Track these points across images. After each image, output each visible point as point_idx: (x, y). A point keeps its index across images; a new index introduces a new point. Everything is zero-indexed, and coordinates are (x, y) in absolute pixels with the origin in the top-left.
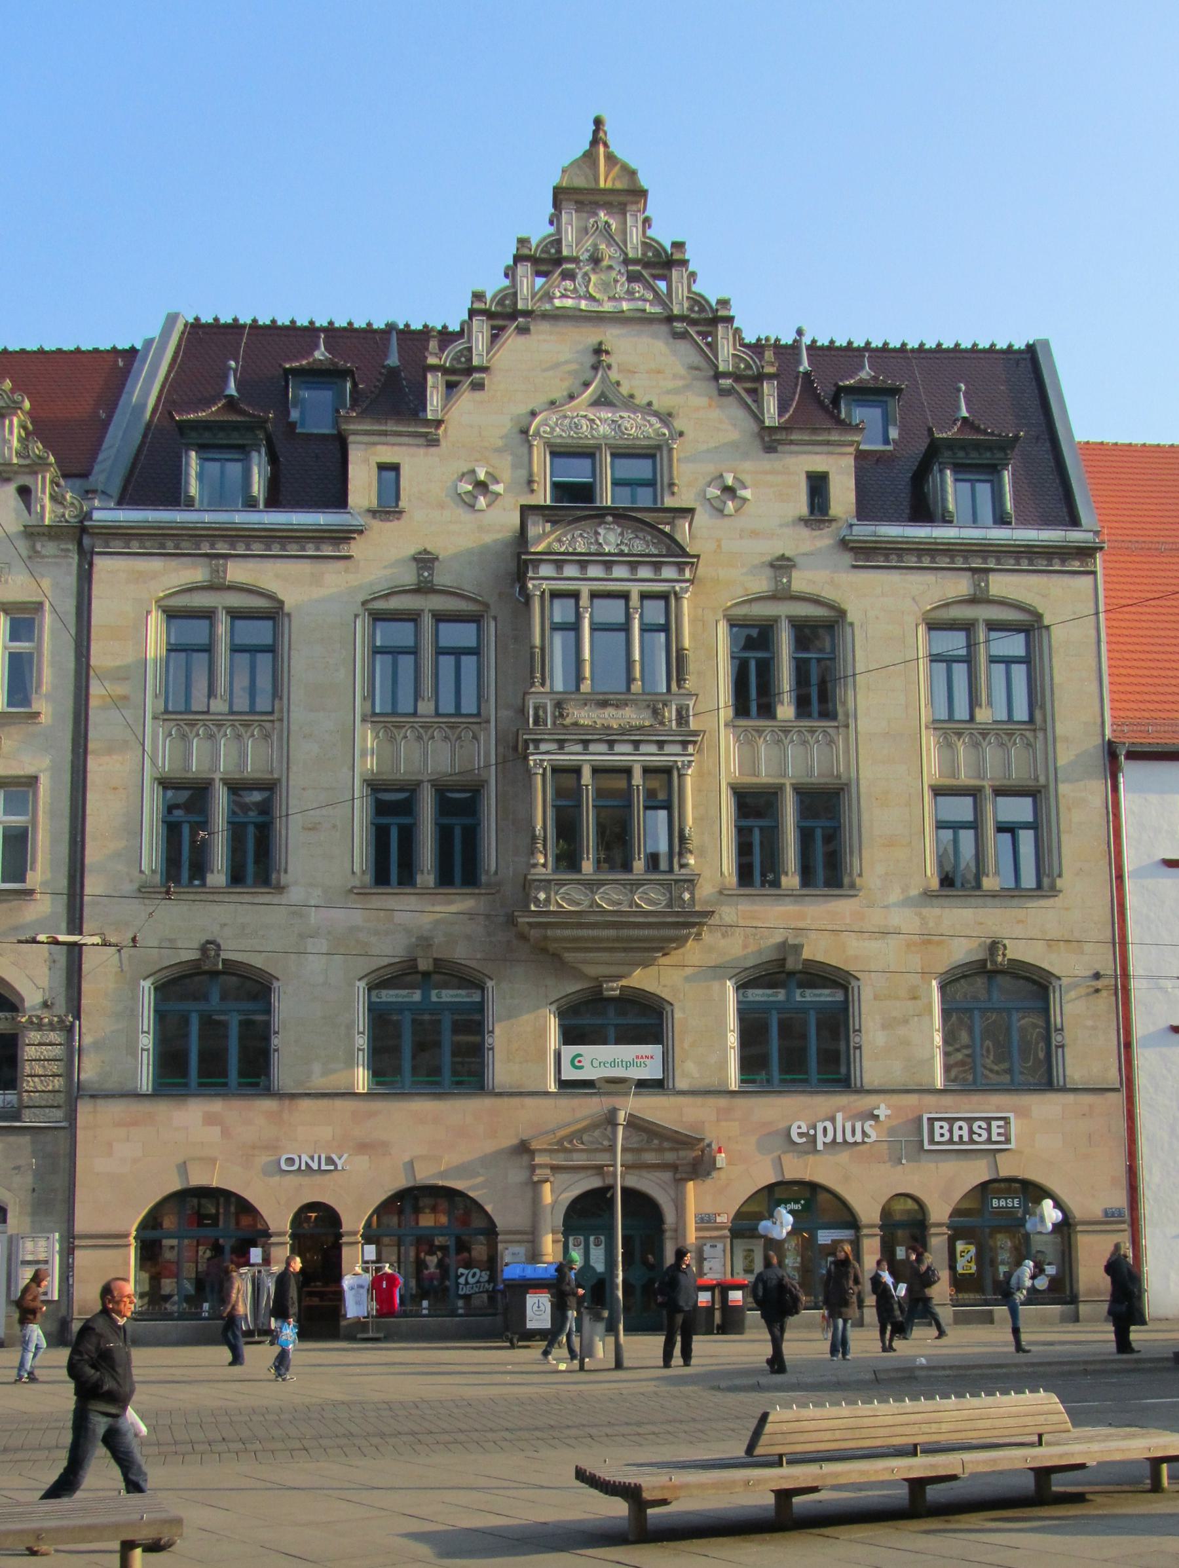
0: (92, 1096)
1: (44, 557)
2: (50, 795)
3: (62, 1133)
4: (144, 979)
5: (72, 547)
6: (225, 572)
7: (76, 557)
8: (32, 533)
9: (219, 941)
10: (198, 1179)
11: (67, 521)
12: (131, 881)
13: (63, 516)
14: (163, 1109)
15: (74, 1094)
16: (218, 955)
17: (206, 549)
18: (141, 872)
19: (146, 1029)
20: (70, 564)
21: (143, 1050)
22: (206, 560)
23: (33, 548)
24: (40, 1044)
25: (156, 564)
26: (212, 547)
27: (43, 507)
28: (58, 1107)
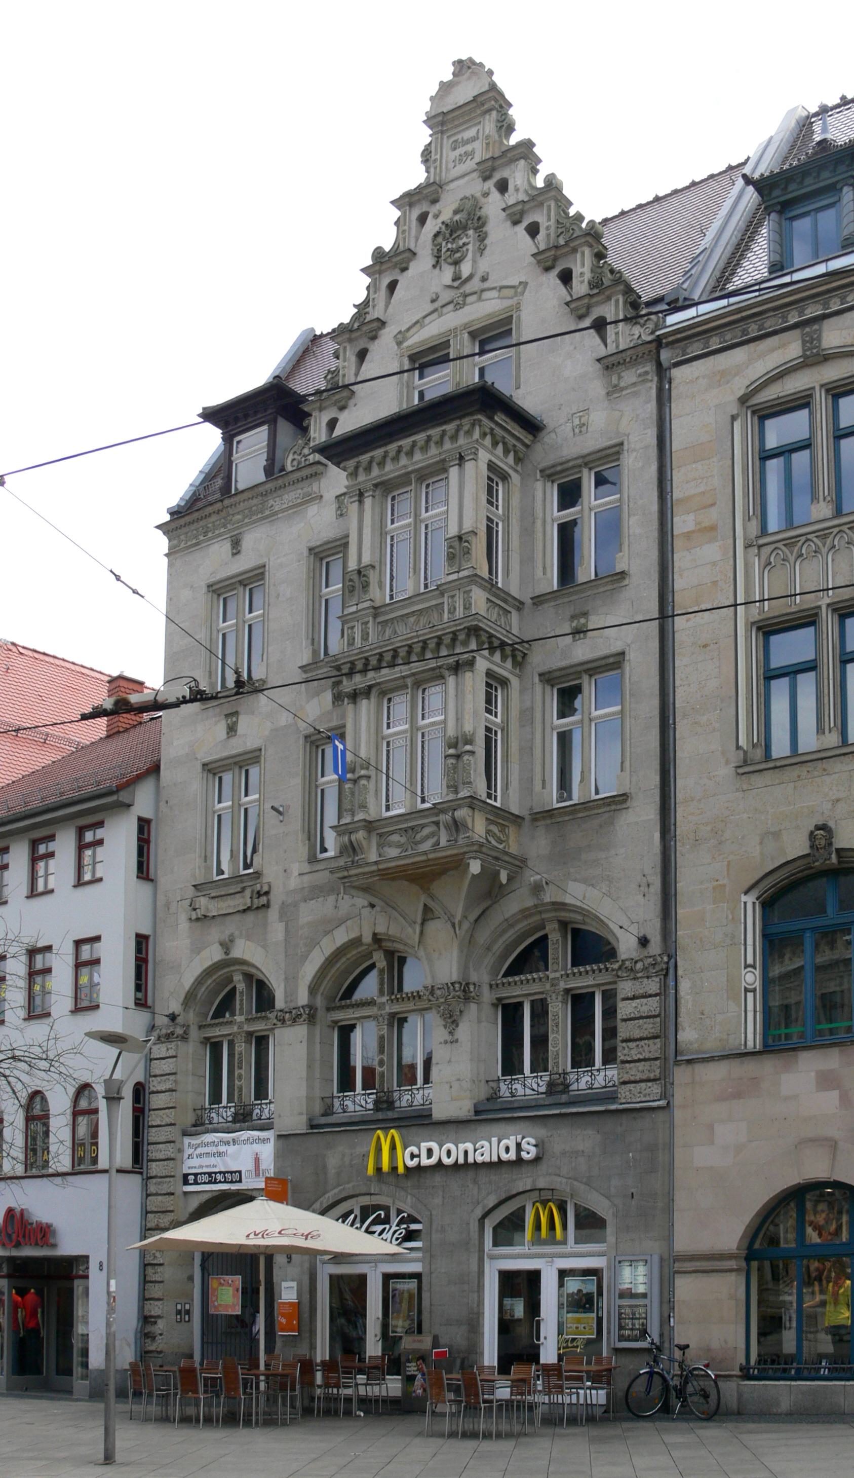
4: (746, 893)
9: (831, 824)
12: (727, 762)
14: (768, 1066)
16: (831, 844)
18: (738, 747)
19: (750, 961)
21: (746, 990)
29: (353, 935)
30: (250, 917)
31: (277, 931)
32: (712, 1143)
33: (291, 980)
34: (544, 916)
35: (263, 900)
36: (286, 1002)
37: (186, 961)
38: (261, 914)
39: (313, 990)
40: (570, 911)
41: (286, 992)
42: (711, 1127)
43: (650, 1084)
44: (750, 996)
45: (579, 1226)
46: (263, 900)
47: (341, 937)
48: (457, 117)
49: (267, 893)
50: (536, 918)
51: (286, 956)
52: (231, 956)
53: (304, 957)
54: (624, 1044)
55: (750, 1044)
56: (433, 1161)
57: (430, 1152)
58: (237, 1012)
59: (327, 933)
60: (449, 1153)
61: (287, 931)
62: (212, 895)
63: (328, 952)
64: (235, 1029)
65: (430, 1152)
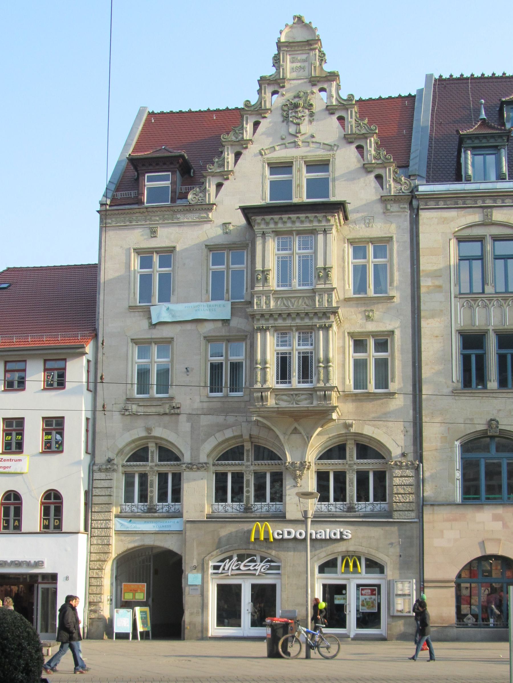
0: (432, 505)
1: (392, 212)
2: (400, 343)
3: (414, 525)
5: (407, 206)
6: (491, 216)
7: (409, 212)
8: (384, 200)
10: (491, 550)
11: (403, 193)
13: (401, 189)
15: (421, 505)
17: (480, 203)
20: (406, 216)
22: (481, 210)
23: (386, 207)
24: (401, 477)
25: (453, 213)
26: (484, 202)
27: (390, 185)
28: (412, 511)
29: (236, 434)
30: (166, 418)
31: (184, 425)
32: (443, 537)
33: (195, 450)
34: (348, 437)
35: (177, 411)
36: (191, 460)
37: (121, 435)
38: (174, 417)
39: (208, 456)
40: (364, 437)
41: (191, 455)
42: (442, 532)
43: (410, 512)
44: (458, 481)
45: (367, 566)
46: (177, 411)
47: (229, 433)
48: (295, 46)
49: (178, 408)
50: (345, 438)
51: (192, 438)
52: (152, 435)
53: (204, 441)
54: (396, 495)
55: (458, 500)
56: (292, 536)
57: (289, 533)
58: (149, 461)
59: (219, 431)
60: (301, 534)
61: (192, 426)
62: (140, 404)
63: (220, 440)
64: (148, 468)
65: (289, 533)
